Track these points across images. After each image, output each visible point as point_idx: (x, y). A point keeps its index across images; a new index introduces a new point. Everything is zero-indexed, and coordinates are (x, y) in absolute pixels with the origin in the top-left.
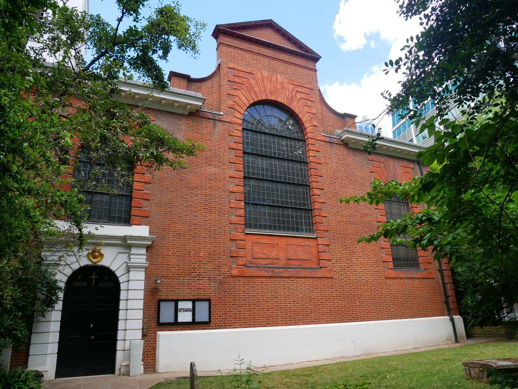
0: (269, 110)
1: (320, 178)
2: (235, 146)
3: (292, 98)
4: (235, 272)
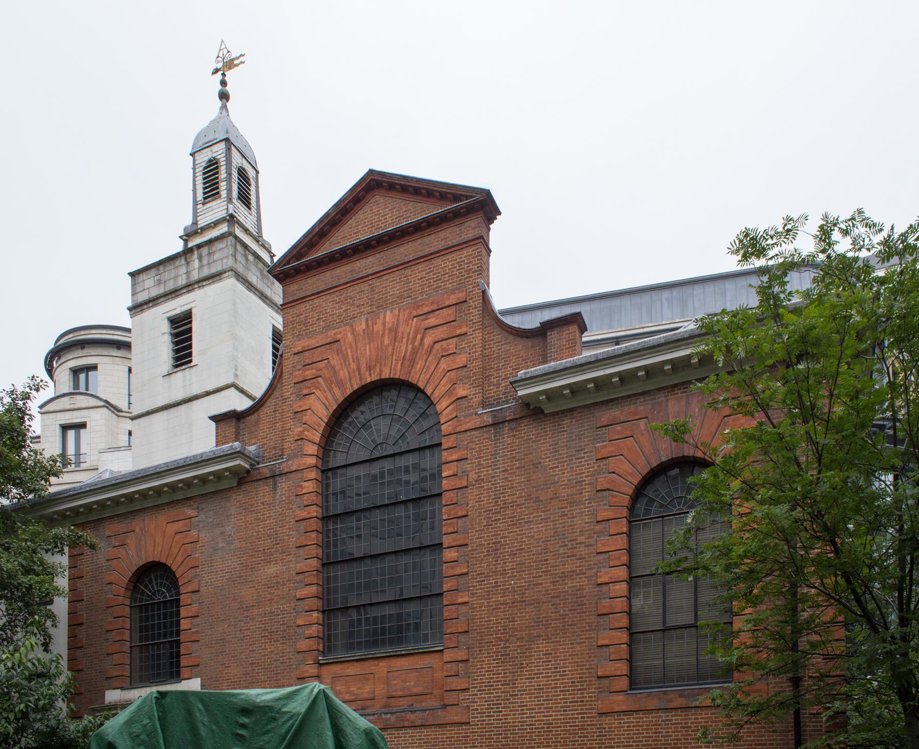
1: (460, 522)
2: (304, 514)
3: (415, 352)
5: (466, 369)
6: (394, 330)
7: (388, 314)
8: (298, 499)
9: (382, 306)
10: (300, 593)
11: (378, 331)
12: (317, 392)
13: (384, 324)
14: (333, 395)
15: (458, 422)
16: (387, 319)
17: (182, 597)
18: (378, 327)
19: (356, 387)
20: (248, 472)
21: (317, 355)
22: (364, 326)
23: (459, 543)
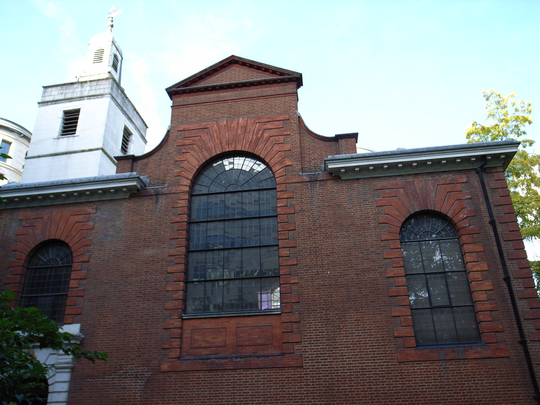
1: (291, 233)
2: (178, 219)
3: (258, 140)
5: (290, 152)
6: (245, 128)
7: (241, 119)
8: (174, 210)
9: (237, 115)
11: (234, 127)
12: (192, 152)
13: (238, 124)
14: (203, 155)
15: (287, 178)
16: (240, 122)
17: (74, 265)
18: (234, 124)
19: (219, 153)
20: (138, 190)
21: (193, 133)
22: (225, 123)
23: (290, 245)
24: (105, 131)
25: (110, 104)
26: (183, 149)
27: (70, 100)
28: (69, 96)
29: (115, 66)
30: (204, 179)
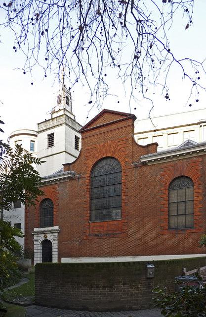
0: (104, 163)
3: (115, 151)
4: (85, 238)
6: (110, 145)
9: (107, 140)
10: (85, 206)
22: (102, 144)
24: (65, 142)
25: (66, 128)
26: (87, 158)
27: (49, 129)
28: (48, 127)
29: (68, 103)
30: (97, 168)
